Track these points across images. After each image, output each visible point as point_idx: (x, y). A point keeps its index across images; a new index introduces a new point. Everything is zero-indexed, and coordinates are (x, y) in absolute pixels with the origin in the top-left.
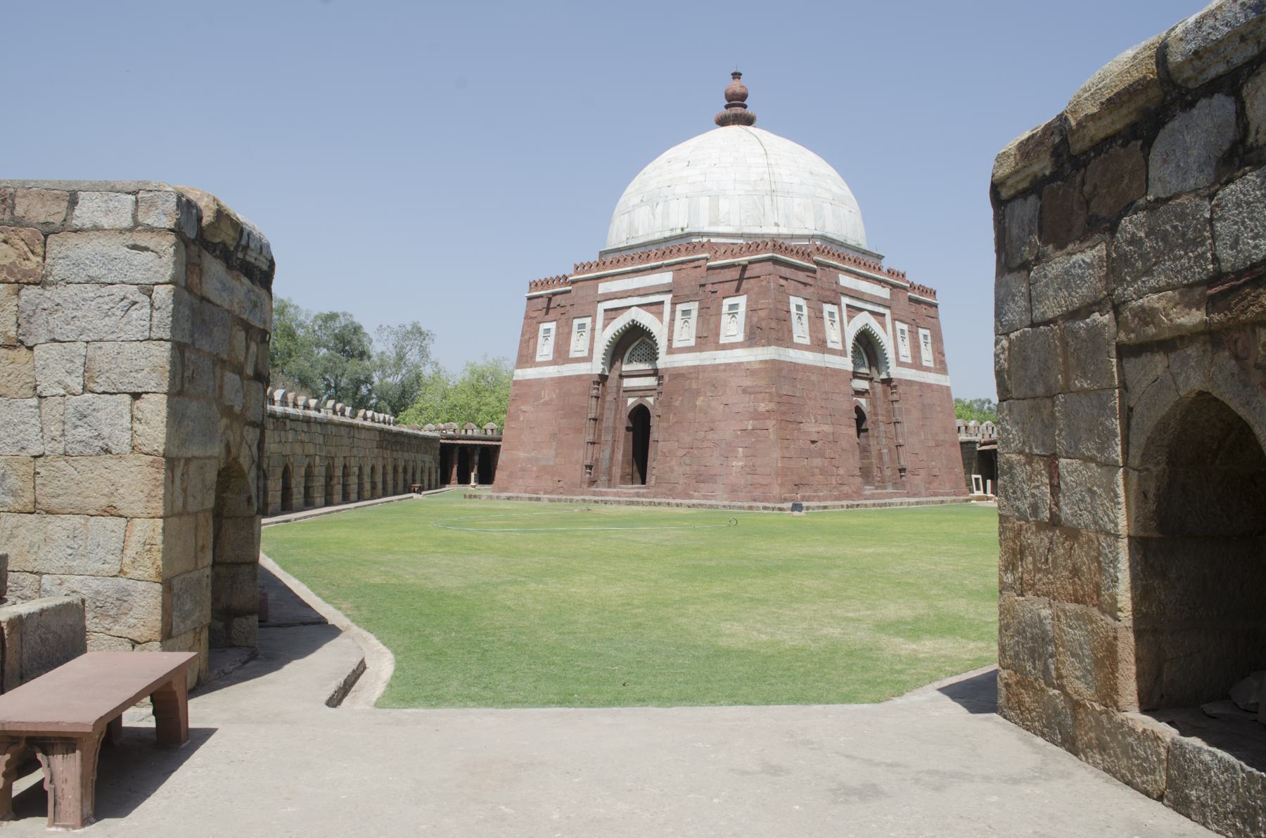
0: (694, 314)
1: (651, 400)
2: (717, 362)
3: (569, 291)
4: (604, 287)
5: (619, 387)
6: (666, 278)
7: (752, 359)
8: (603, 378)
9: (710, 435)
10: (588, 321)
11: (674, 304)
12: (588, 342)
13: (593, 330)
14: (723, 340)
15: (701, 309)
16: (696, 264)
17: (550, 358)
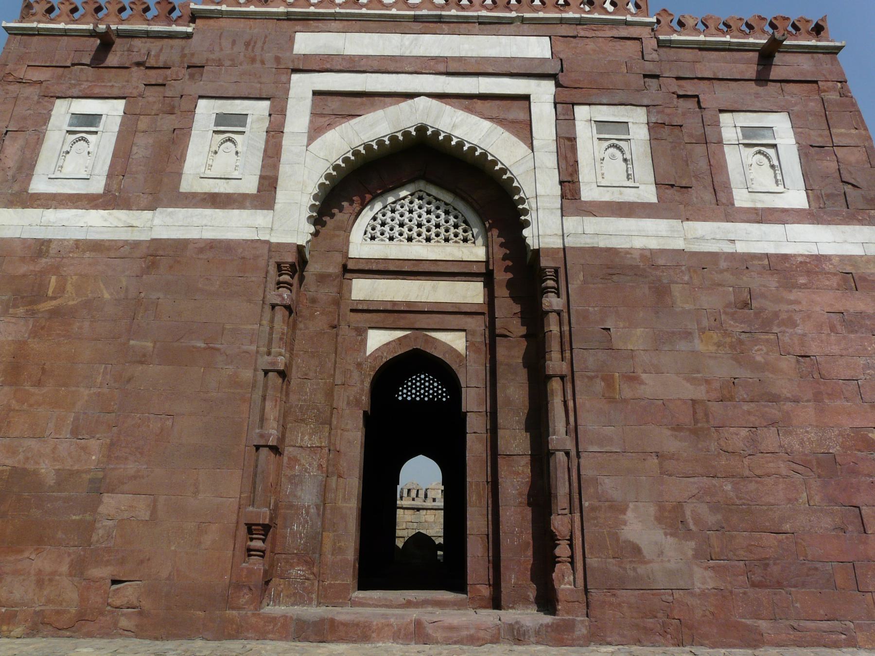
0: (639, 133)
1: (456, 341)
2: (741, 248)
3: (188, 36)
4: (306, 43)
5: (343, 291)
6: (537, 47)
7: (857, 251)
8: (295, 265)
9: (770, 439)
10: (258, 110)
11: (564, 107)
12: (256, 161)
13: (275, 133)
14: (741, 199)
15: (652, 127)
16: (624, 32)
17: (97, 186)
